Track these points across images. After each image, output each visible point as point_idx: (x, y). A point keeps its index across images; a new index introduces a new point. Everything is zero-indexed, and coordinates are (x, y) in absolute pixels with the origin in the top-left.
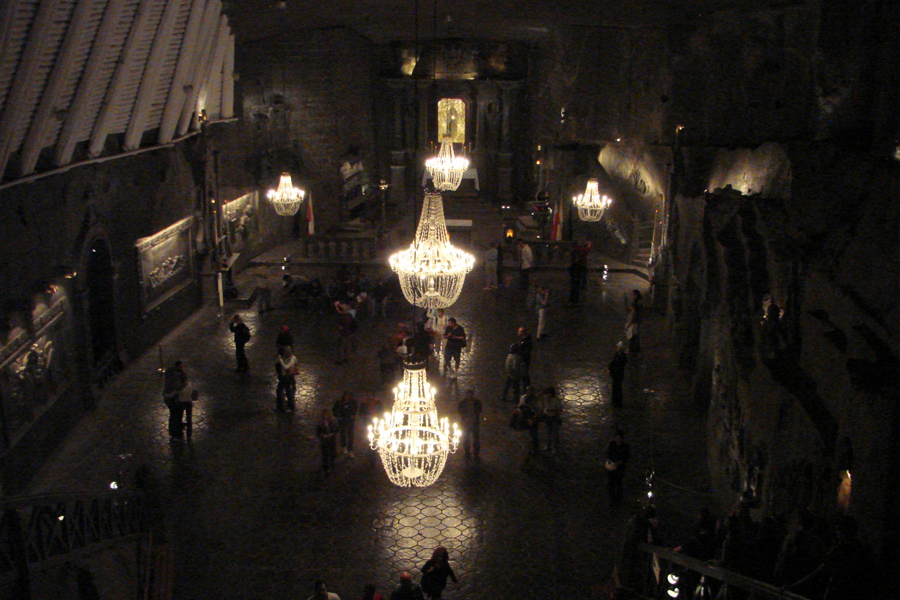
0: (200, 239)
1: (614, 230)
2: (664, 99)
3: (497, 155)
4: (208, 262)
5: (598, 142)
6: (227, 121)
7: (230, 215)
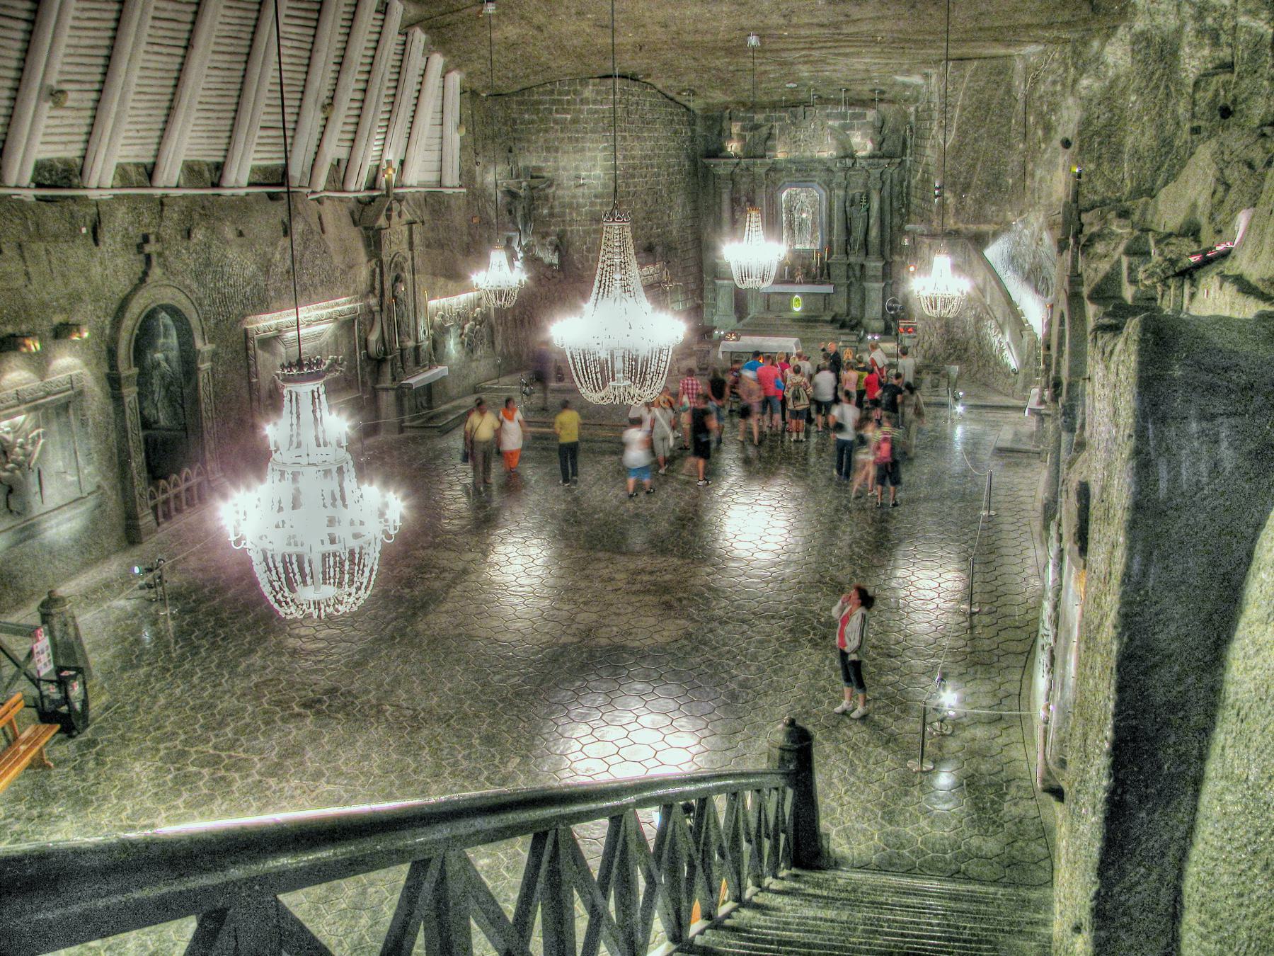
0: (374, 337)
1: (1002, 351)
2: (1066, 144)
3: (862, 266)
4: (387, 369)
5: (984, 228)
6: (450, 191)
7: (442, 317)
